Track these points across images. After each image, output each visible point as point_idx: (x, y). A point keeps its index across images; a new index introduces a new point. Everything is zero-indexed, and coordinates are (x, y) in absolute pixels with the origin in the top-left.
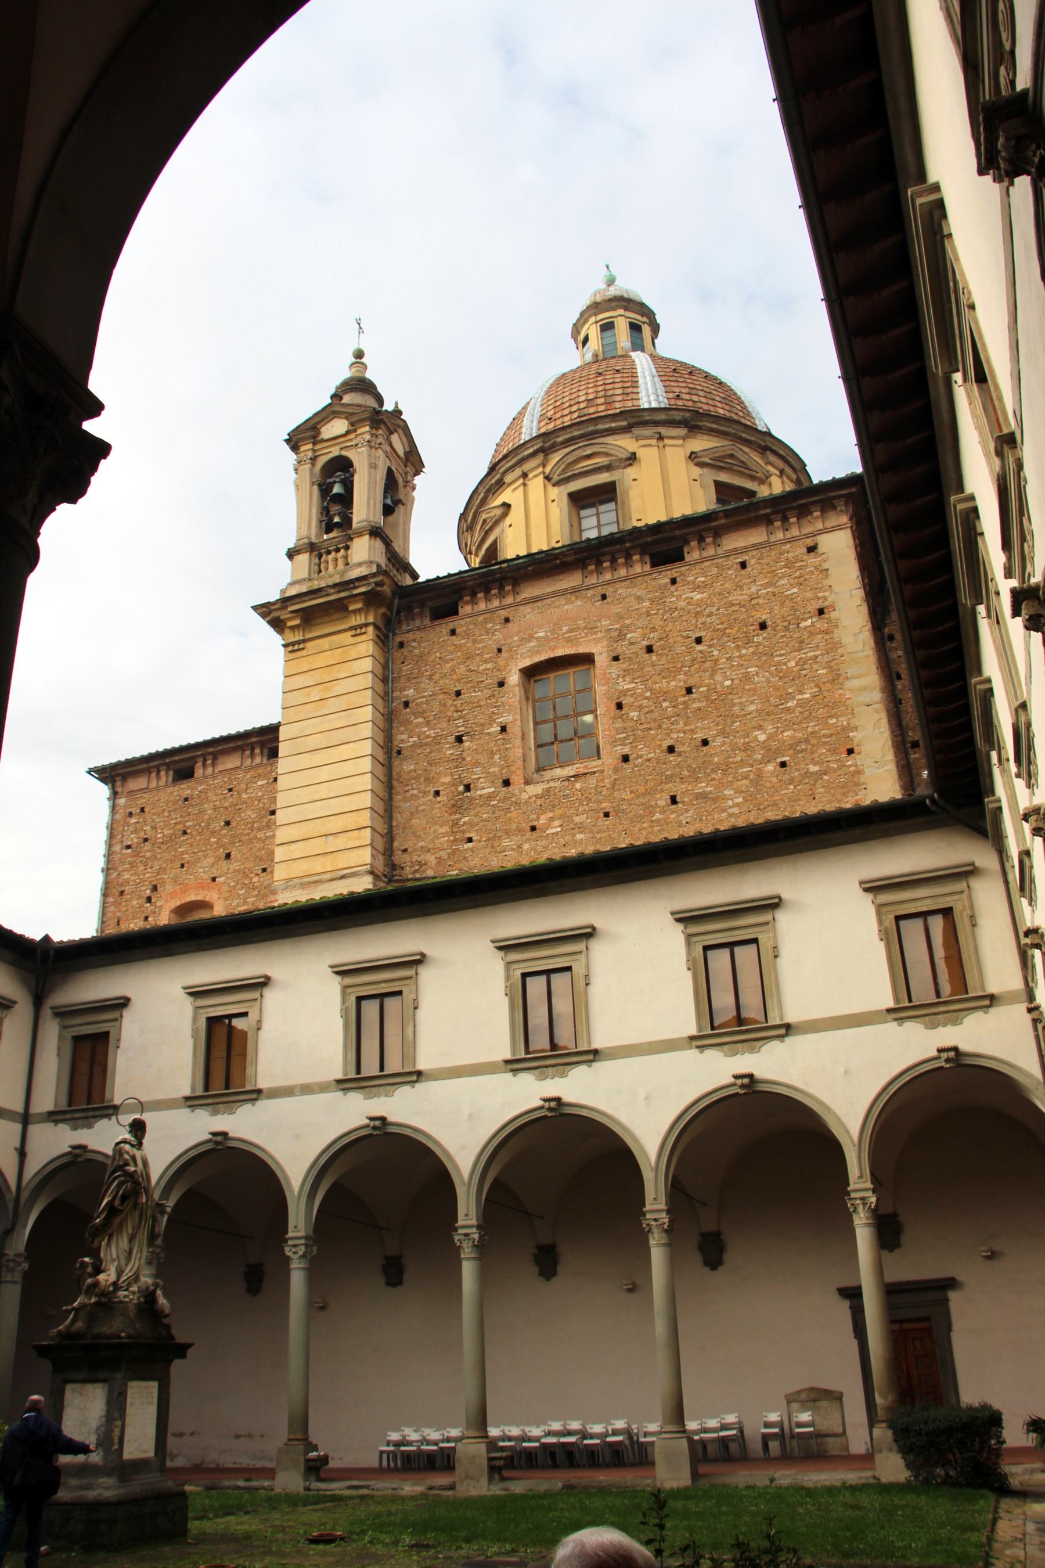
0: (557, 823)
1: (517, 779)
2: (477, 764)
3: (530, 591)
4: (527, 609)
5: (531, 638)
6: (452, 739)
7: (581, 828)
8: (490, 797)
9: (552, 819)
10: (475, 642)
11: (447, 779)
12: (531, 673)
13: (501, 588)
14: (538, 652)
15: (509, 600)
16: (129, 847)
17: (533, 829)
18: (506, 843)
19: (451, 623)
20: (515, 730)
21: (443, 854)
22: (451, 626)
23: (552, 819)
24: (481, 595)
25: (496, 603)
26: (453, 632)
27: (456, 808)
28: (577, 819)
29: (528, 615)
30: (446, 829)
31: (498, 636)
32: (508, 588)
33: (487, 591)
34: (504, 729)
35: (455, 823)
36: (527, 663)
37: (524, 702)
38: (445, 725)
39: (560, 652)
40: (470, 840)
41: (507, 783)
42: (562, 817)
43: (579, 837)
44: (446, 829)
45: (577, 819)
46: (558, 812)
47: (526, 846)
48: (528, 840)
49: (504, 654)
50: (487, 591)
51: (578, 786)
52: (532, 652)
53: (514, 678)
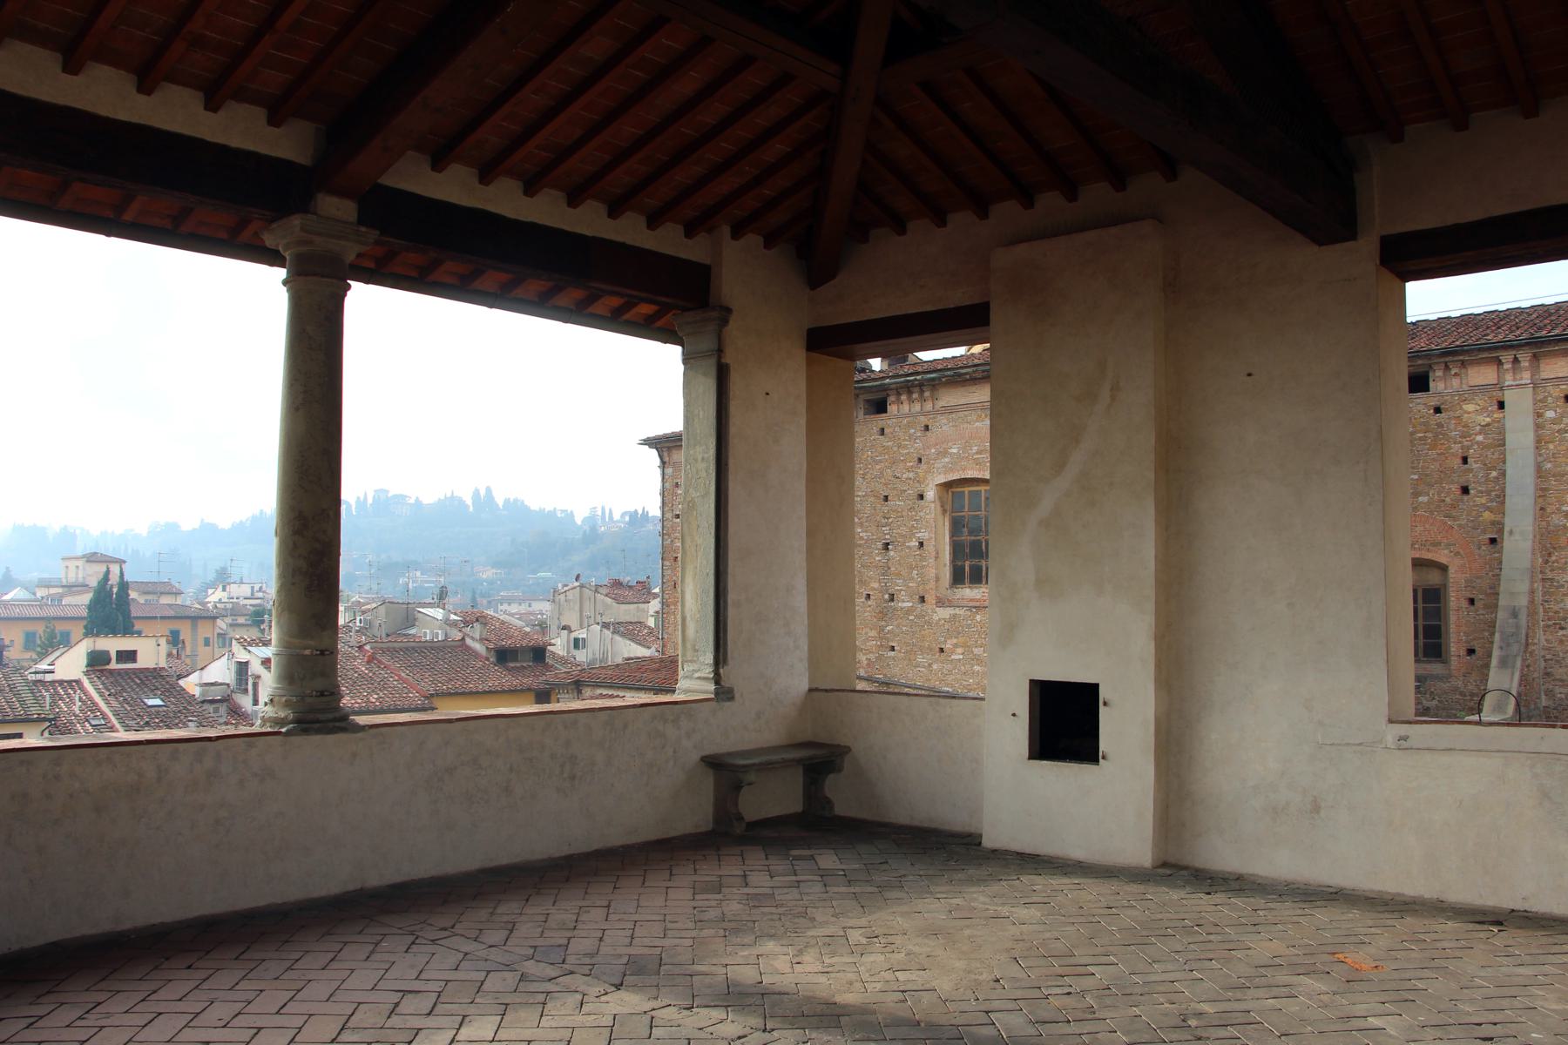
0: (960, 650)
1: (930, 599)
2: (899, 575)
3: (949, 398)
4: (943, 420)
5: (945, 453)
6: (880, 545)
7: (979, 661)
8: (909, 611)
9: (956, 646)
10: (899, 446)
11: (876, 585)
12: (948, 485)
13: (922, 392)
14: (952, 470)
15: (928, 406)
16: (678, 516)
17: (942, 650)
18: (920, 659)
19: (880, 420)
20: (930, 547)
21: (872, 657)
22: (881, 424)
23: (956, 646)
24: (903, 397)
25: (917, 407)
26: (882, 432)
27: (883, 615)
28: (976, 651)
29: (943, 426)
30: (873, 633)
31: (919, 445)
32: (927, 394)
33: (910, 393)
34: (921, 544)
35: (882, 629)
36: (942, 479)
37: (940, 517)
38: (874, 529)
39: (970, 474)
40: (893, 649)
41: (922, 599)
42: (964, 645)
43: (976, 668)
44: (873, 633)
45: (976, 651)
46: (961, 640)
47: (935, 666)
48: (936, 661)
49: (923, 466)
50: (910, 393)
51: (978, 618)
52: (948, 470)
53: (930, 494)
